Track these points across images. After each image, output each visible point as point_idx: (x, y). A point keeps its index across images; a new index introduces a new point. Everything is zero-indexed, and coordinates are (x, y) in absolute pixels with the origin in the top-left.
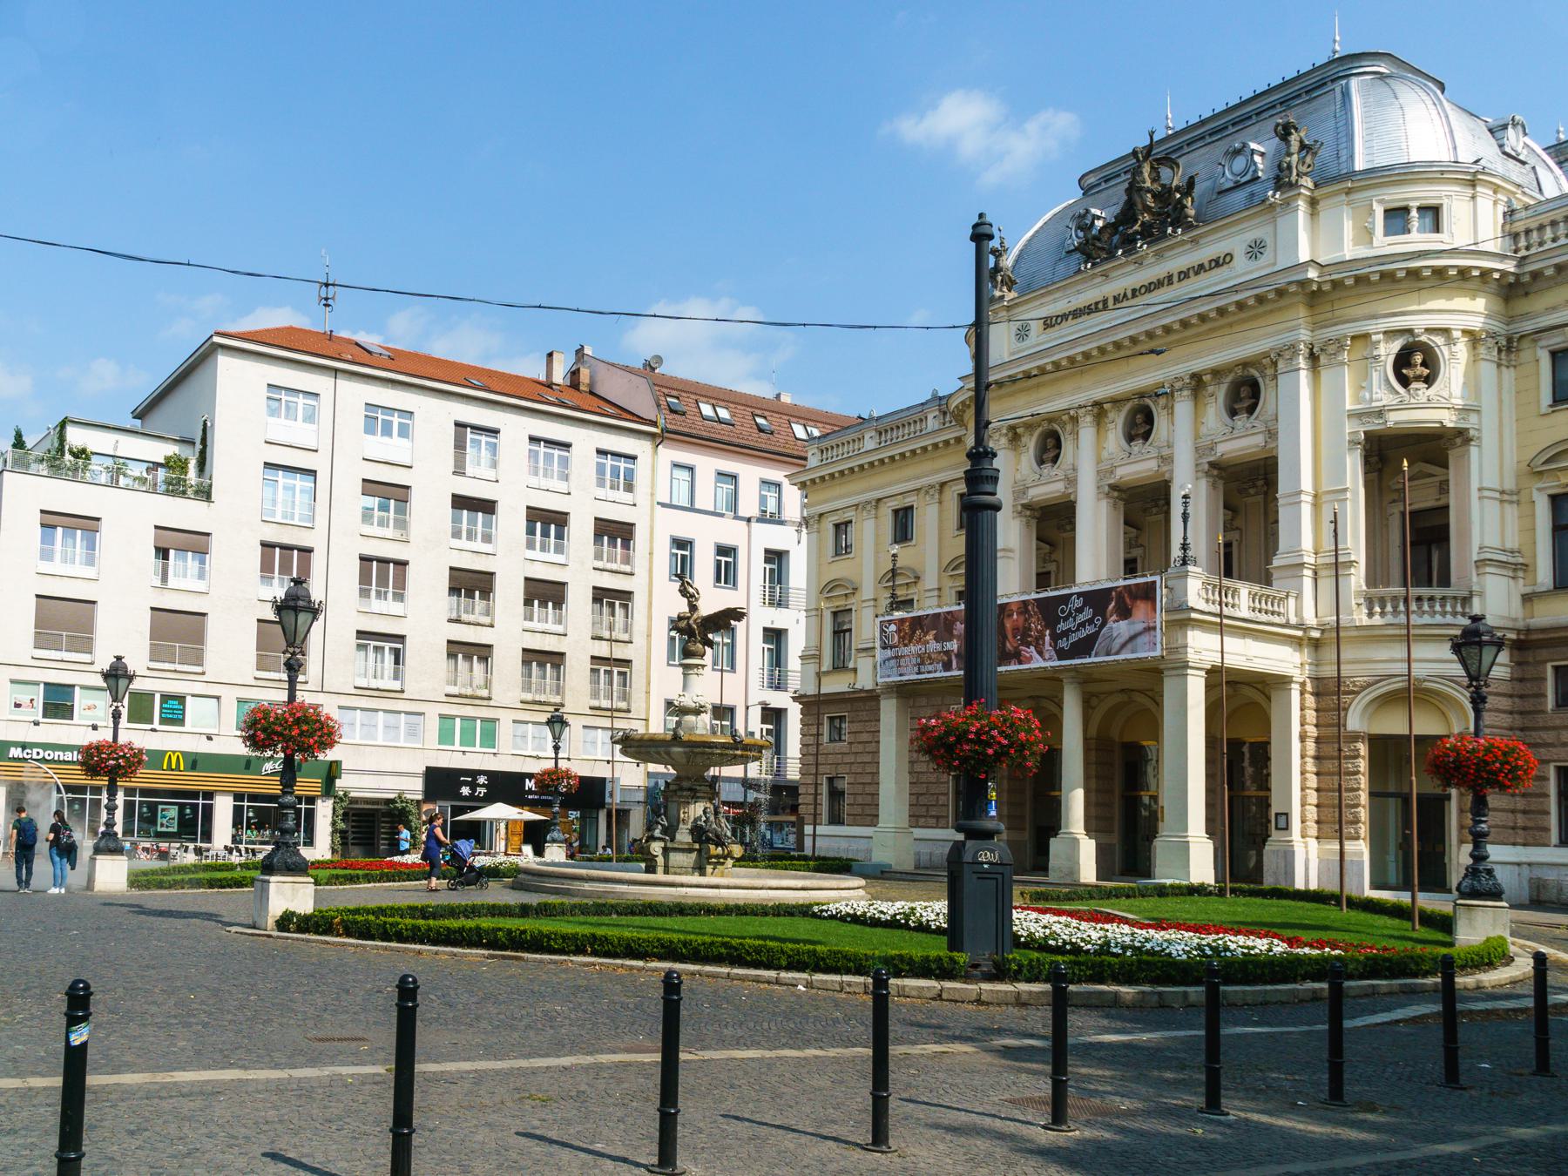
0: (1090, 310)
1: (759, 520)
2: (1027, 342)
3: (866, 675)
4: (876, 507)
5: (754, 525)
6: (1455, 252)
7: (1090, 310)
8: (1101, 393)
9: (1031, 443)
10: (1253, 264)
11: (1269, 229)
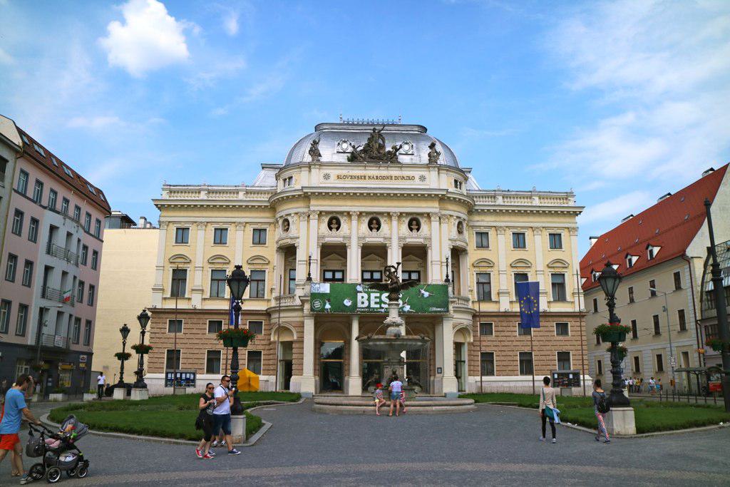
0: (359, 178)
1: (51, 210)
2: (328, 181)
3: (195, 301)
4: (206, 226)
5: (48, 212)
6: (534, 206)
7: (359, 178)
8: (363, 209)
9: (326, 220)
10: (421, 183)
11: (428, 173)
